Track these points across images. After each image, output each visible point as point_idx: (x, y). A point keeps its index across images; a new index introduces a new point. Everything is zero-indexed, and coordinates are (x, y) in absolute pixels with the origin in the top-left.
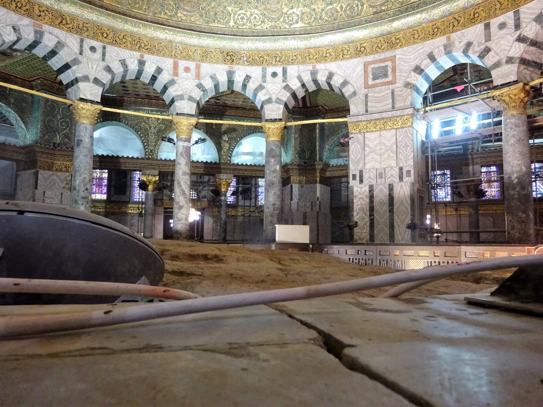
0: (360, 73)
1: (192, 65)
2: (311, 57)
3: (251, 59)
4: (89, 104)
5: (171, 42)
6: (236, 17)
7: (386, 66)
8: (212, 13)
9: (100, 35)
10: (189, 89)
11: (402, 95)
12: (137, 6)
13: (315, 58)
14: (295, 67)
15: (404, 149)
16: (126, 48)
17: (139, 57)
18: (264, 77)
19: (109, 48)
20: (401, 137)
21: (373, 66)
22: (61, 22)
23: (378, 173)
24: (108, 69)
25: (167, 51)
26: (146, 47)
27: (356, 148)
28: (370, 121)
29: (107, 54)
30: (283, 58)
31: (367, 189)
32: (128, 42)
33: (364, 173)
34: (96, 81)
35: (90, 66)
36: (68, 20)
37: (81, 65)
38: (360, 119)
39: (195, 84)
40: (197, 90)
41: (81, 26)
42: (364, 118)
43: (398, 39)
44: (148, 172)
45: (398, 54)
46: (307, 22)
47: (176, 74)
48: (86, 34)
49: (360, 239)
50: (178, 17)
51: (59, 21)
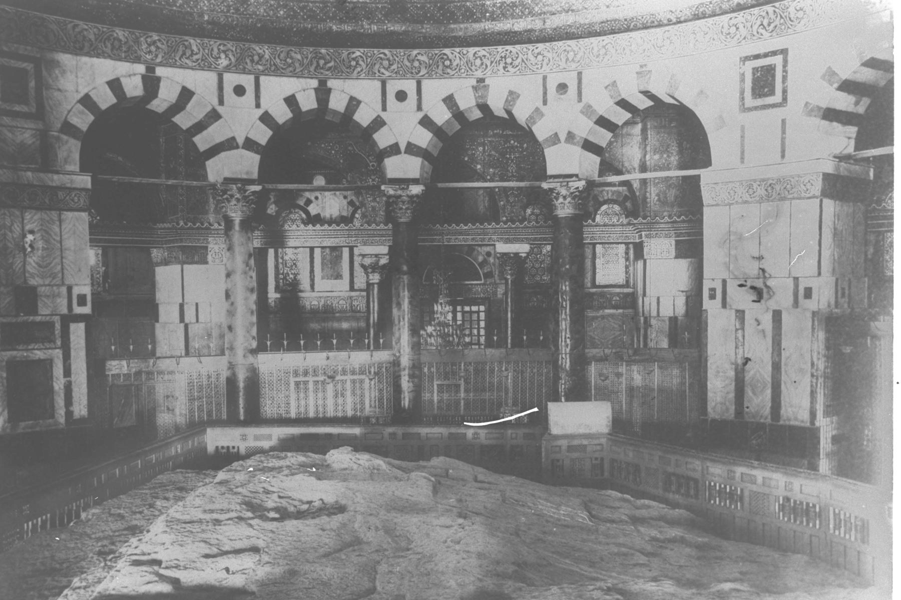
1: (409, 86)
24: (266, 118)
25: (364, 66)
32: (297, 65)
34: (250, 144)
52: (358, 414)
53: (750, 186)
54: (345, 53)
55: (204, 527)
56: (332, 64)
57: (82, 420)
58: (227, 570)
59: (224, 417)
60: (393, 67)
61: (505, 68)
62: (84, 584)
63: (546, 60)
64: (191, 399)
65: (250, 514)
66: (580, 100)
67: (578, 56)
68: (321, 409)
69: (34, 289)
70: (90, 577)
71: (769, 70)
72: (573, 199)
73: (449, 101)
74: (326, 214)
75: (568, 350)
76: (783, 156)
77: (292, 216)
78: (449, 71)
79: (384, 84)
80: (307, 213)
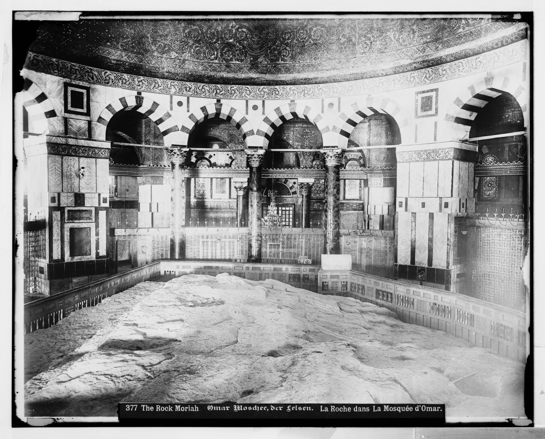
9: (184, 90)
12: (213, 56)
24: (191, 117)
25: (238, 93)
32: (207, 92)
34: (184, 129)
43: (445, 70)
51: (153, 86)
52: (232, 257)
53: (419, 154)
54: (229, 87)
55: (158, 309)
56: (223, 92)
57: (102, 257)
58: (168, 330)
59: (169, 257)
60: (251, 94)
61: (304, 95)
62: (102, 333)
63: (324, 92)
64: (154, 249)
65: (179, 303)
66: (339, 111)
67: (339, 91)
68: (214, 254)
69: (83, 195)
70: (105, 331)
71: (429, 98)
72: (336, 157)
73: (278, 110)
74: (219, 163)
75: (331, 230)
76: (435, 140)
77: (203, 163)
78: (277, 96)
79: (247, 101)
80: (210, 162)
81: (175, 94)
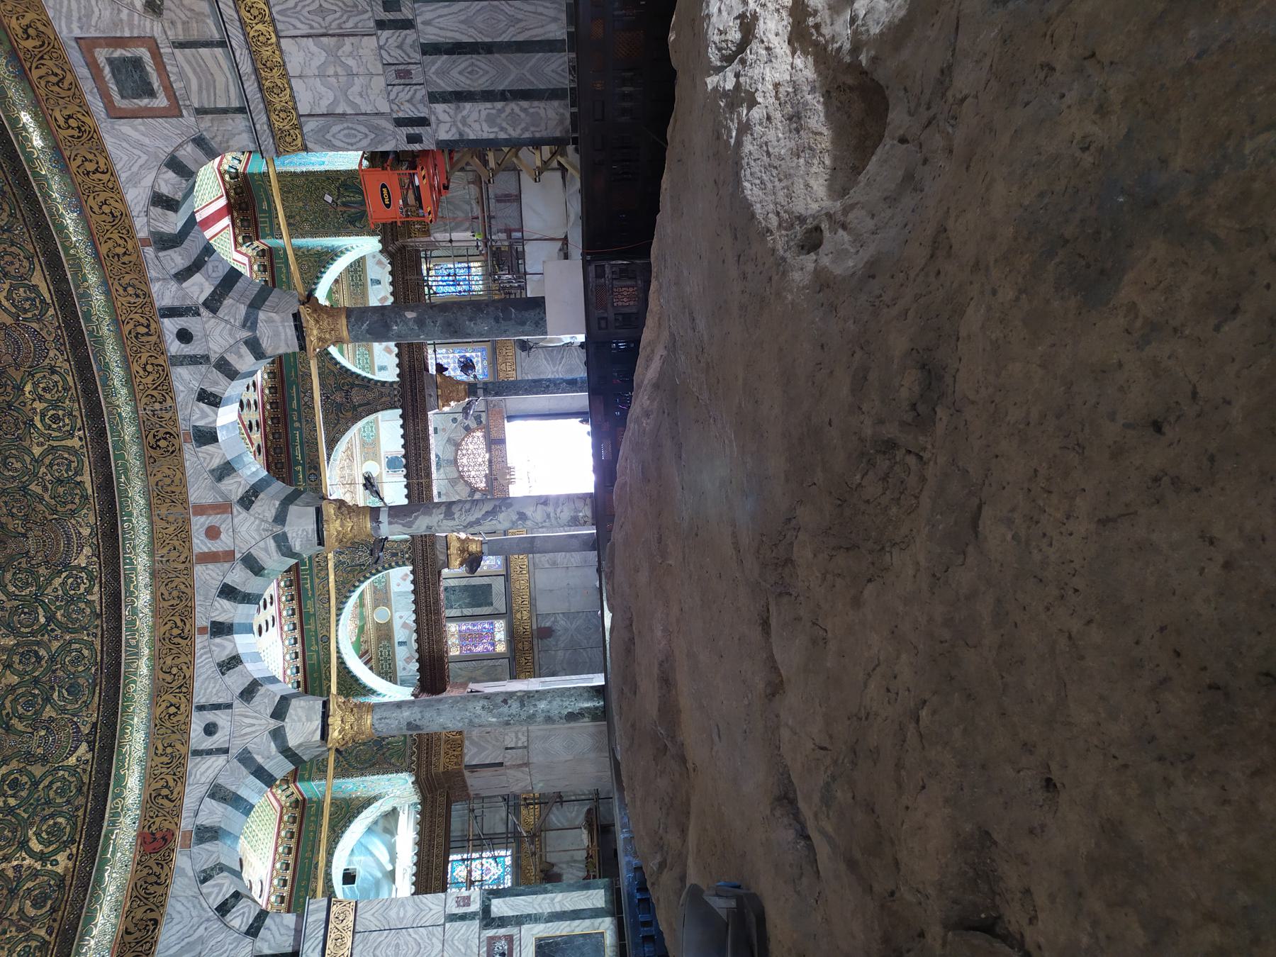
0: (142, 128)
1: (199, 524)
2: (120, 251)
3: (155, 393)
4: (330, 720)
5: (153, 574)
6: (54, 434)
7: (110, 61)
8: (61, 490)
9: (175, 719)
10: (259, 526)
11: (184, 23)
12: (86, 653)
13: (121, 242)
14: (155, 288)
15: (329, 19)
16: (190, 664)
17: (206, 636)
18: (194, 360)
19: (199, 699)
20: (299, 25)
21: (116, 97)
22: (167, 796)
23: (397, 81)
26: (179, 623)
27: (340, 136)
28: (268, 105)
29: (214, 700)
30: (137, 317)
31: (439, 108)
32: (177, 661)
33: (401, 115)
35: (248, 730)
36: (159, 785)
37: (251, 747)
38: (265, 127)
39: (244, 514)
40: (256, 507)
41: (165, 759)
42: (261, 120)
43: (25, 31)
44: (442, 557)
45: (71, 31)
46: (26, 263)
47: (229, 556)
48: (178, 746)
49: (561, 122)
50: (89, 564)
51: (165, 802)
67: (142, 321)
81: (186, 742)
